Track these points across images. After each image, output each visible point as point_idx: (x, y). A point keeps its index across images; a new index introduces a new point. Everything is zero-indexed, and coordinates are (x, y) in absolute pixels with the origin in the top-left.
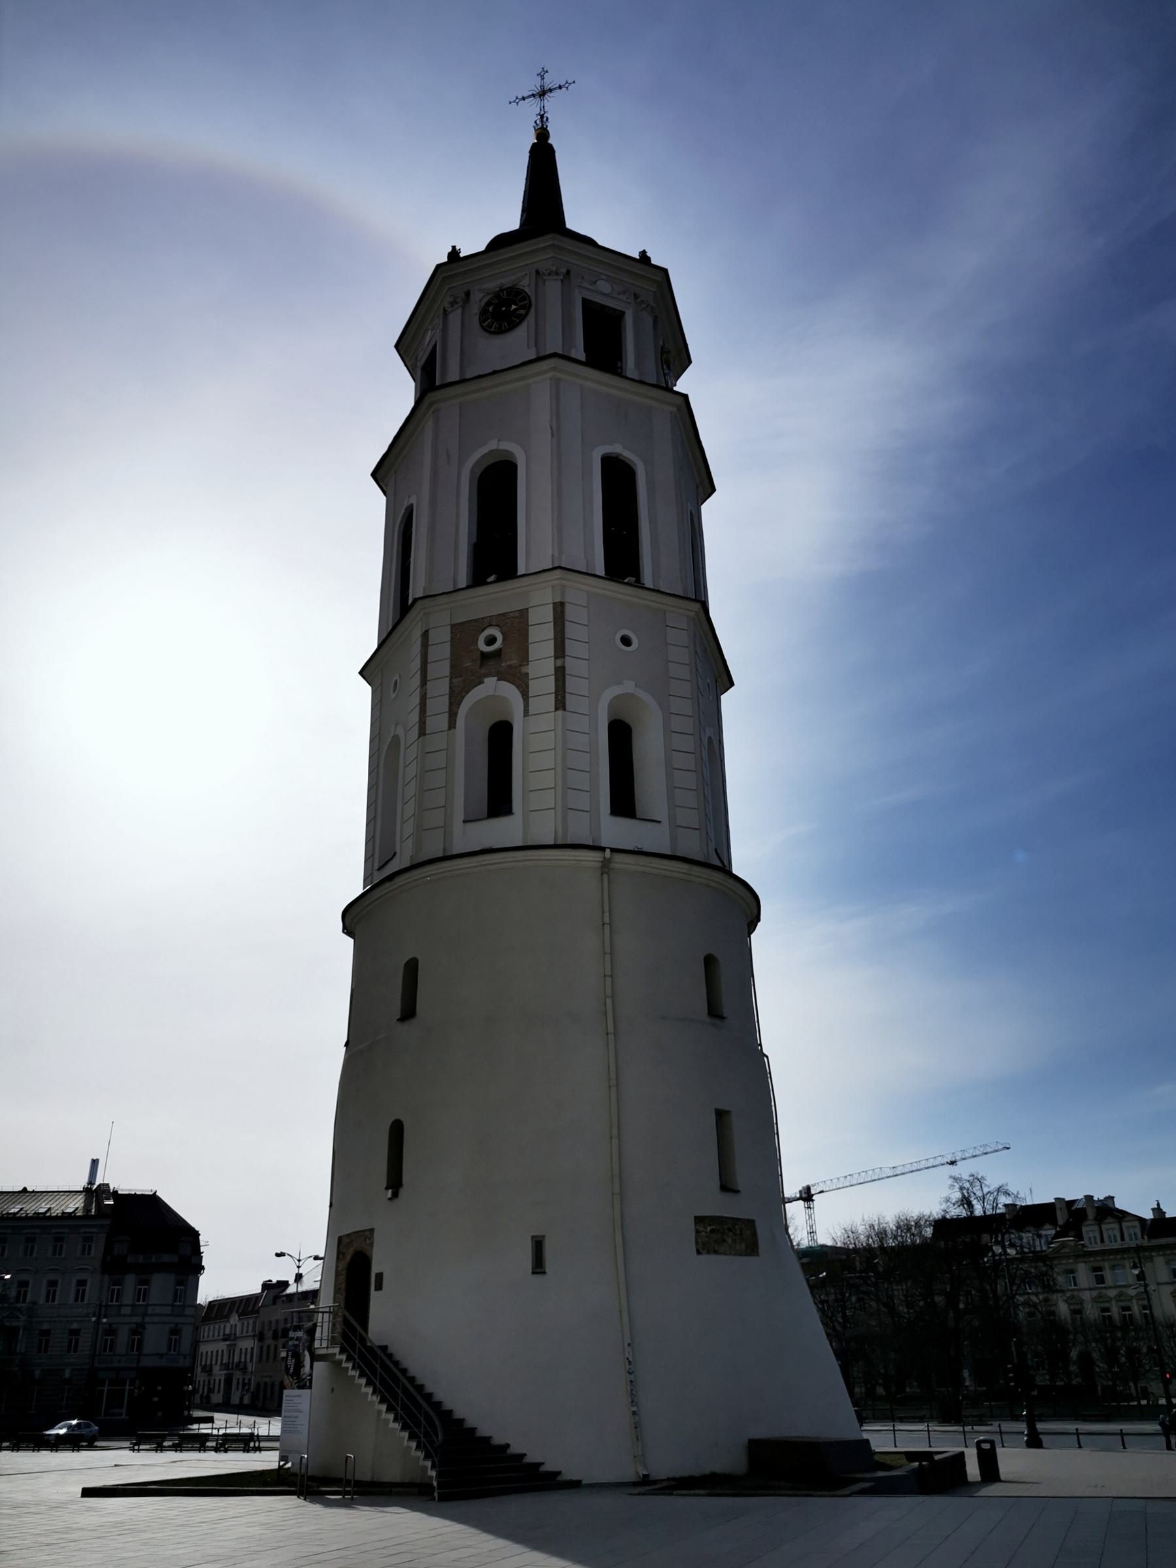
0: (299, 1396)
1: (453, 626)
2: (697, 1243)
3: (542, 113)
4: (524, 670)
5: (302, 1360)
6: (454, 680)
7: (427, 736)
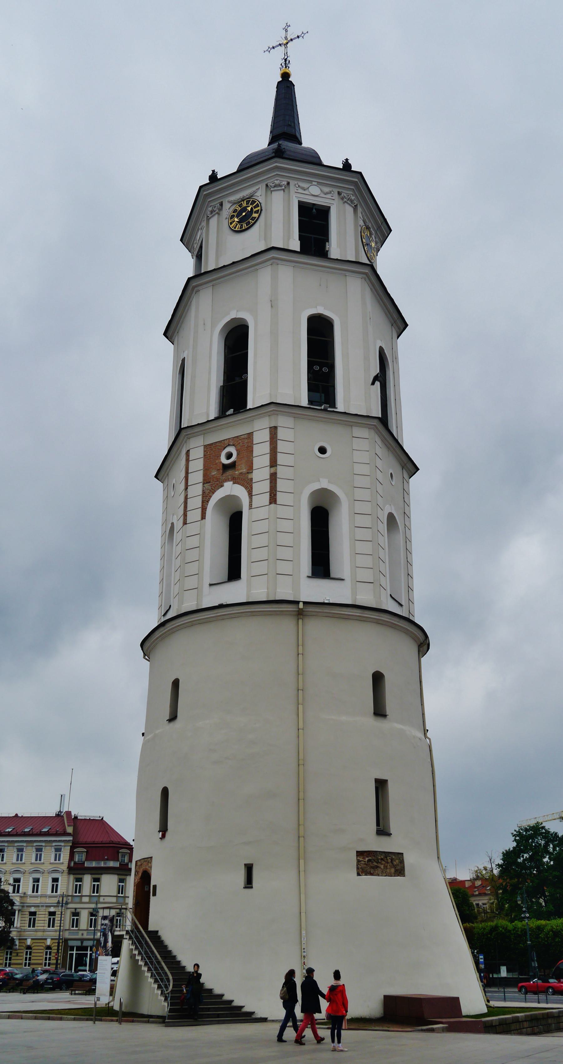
0: (106, 960)
1: (205, 446)
2: (358, 868)
3: (286, 57)
4: (250, 476)
5: (107, 938)
6: (205, 485)
7: (187, 525)
